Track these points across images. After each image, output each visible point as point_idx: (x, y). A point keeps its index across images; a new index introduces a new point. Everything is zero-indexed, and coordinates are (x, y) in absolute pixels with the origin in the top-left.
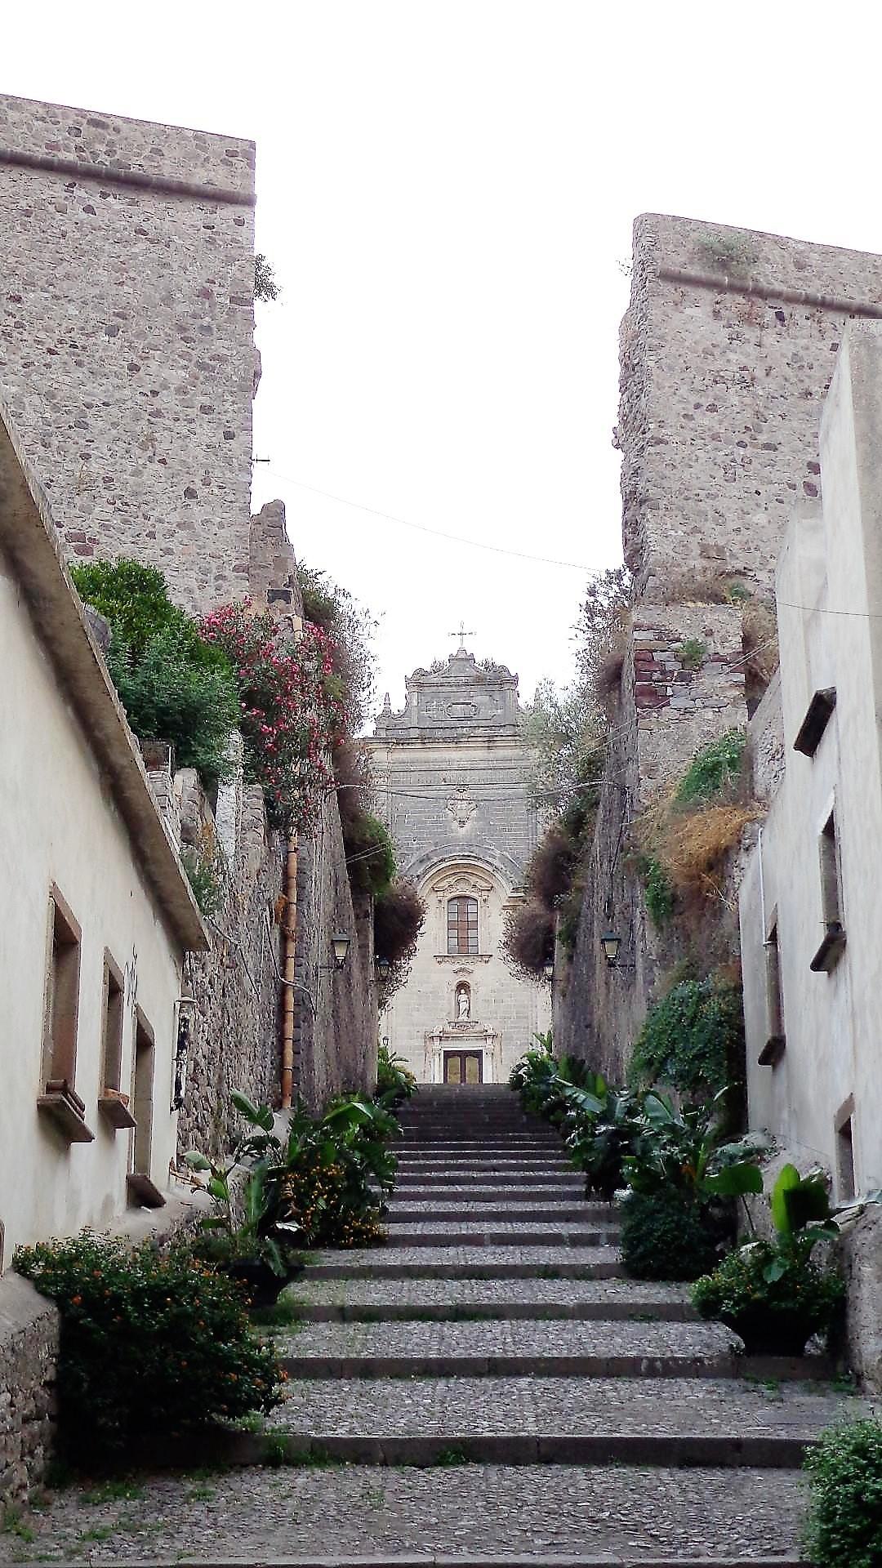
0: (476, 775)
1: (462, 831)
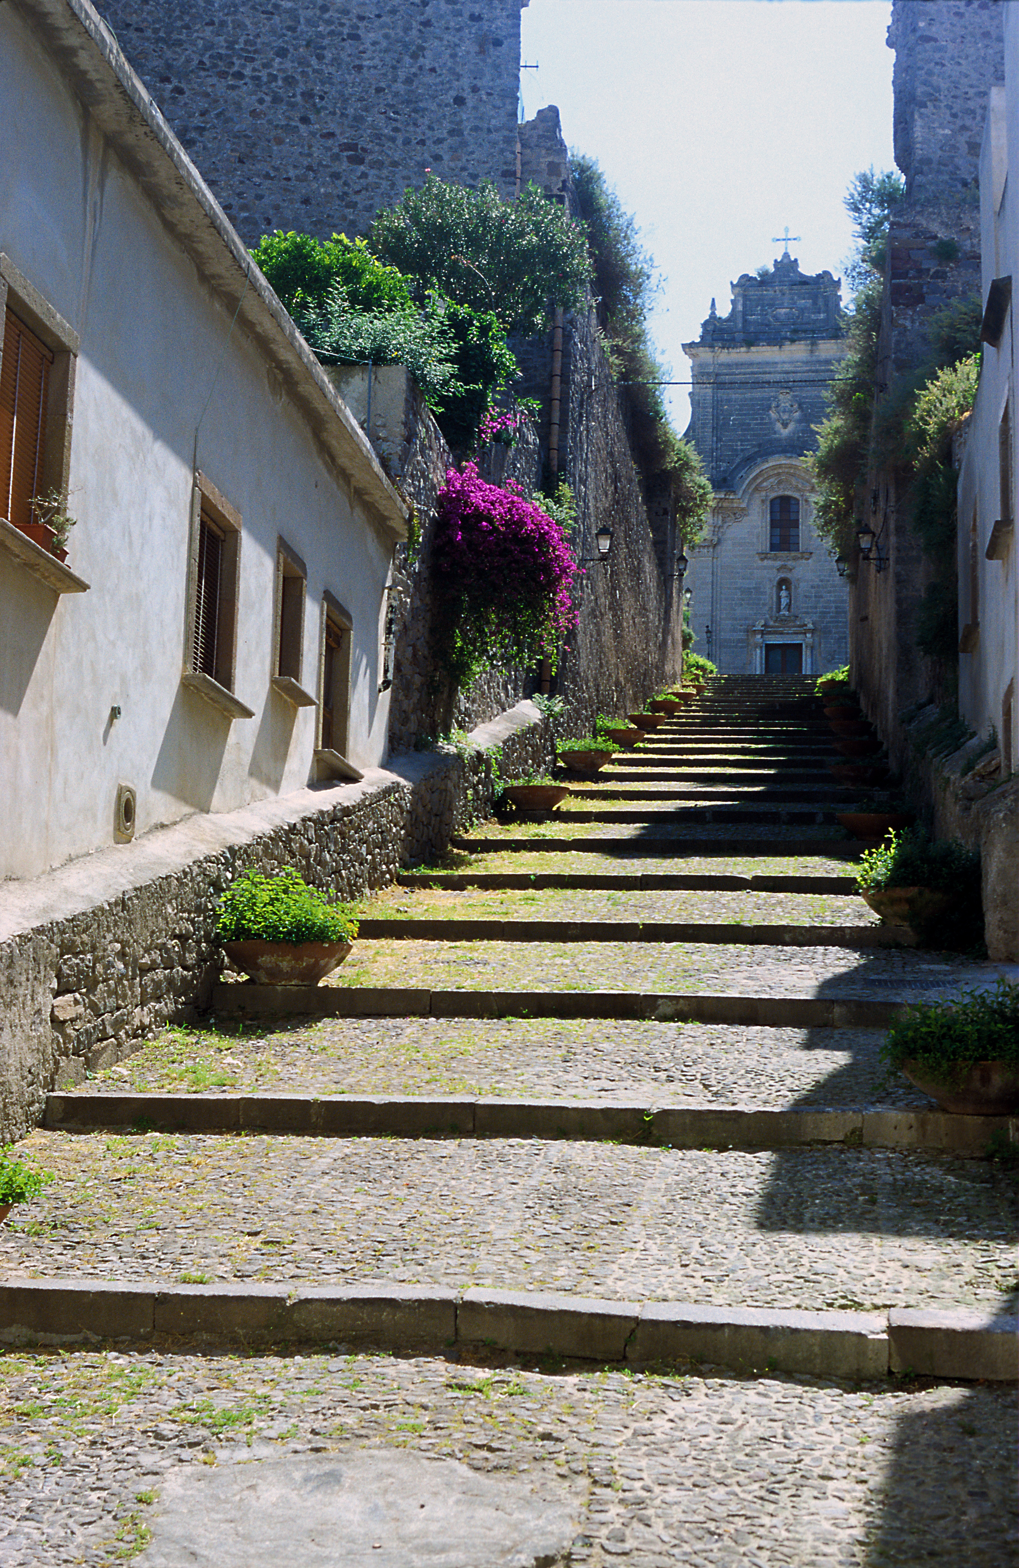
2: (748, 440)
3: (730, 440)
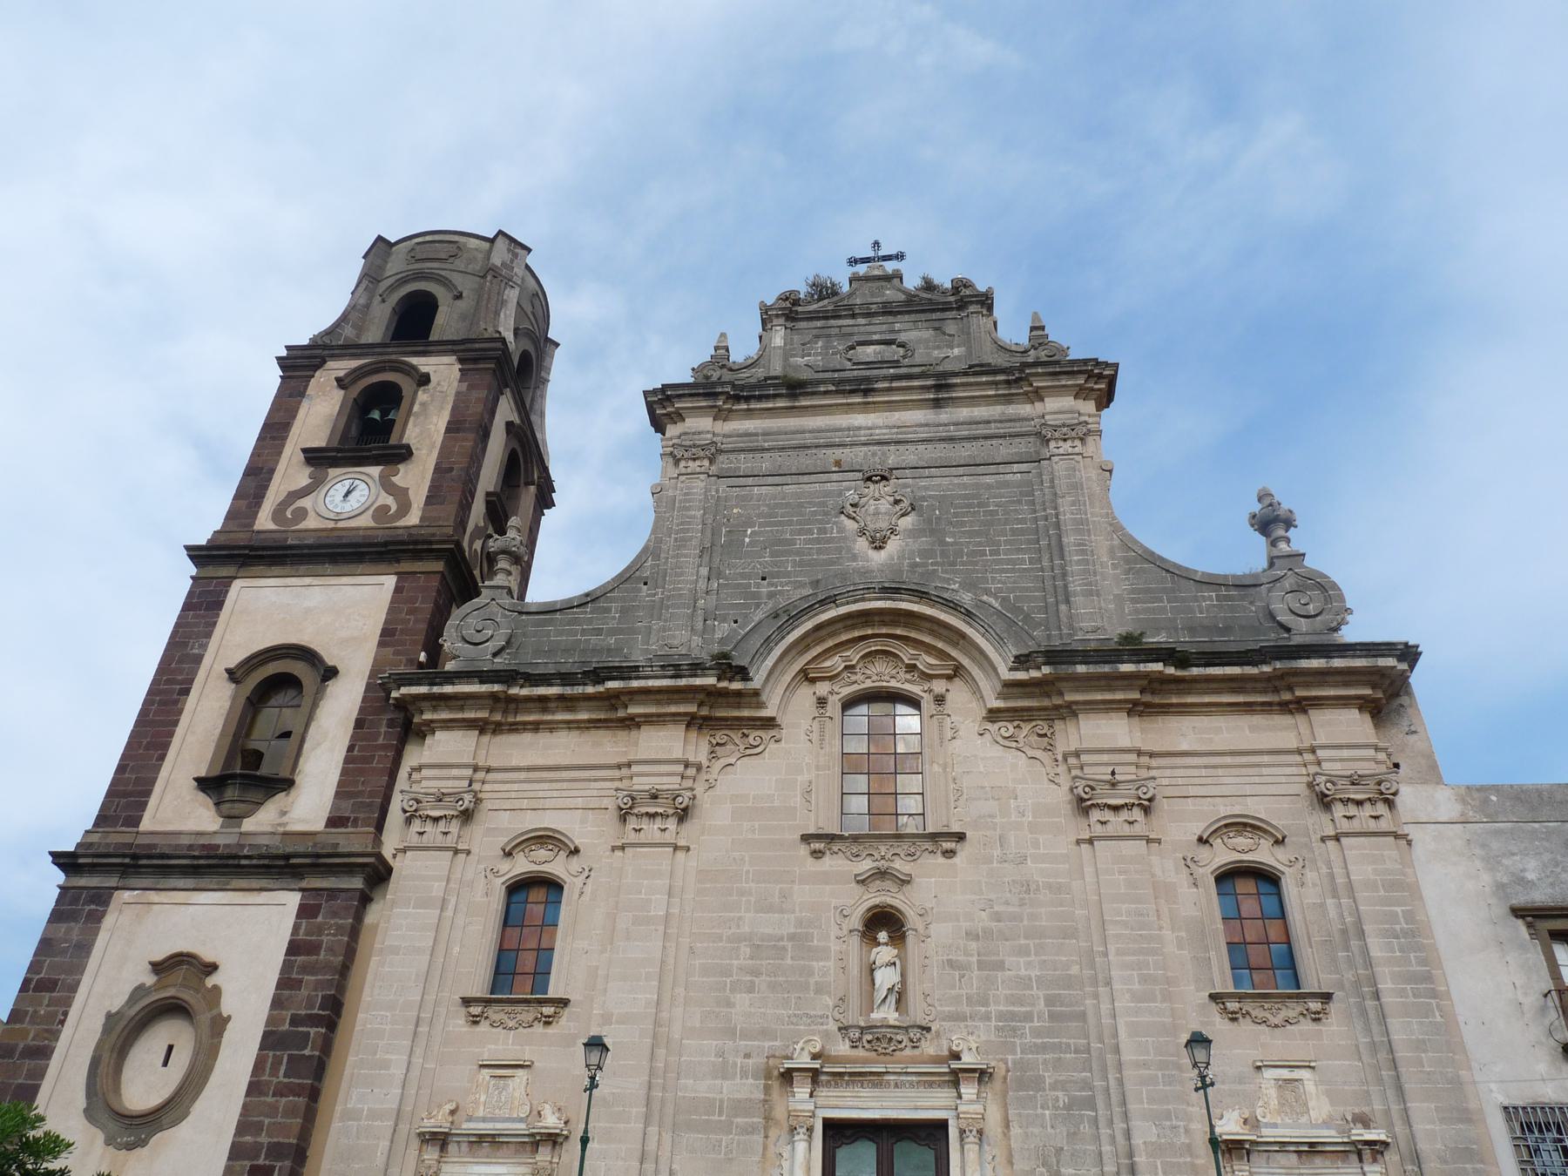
0: (910, 455)
1: (878, 558)
2: (788, 574)
3: (743, 576)
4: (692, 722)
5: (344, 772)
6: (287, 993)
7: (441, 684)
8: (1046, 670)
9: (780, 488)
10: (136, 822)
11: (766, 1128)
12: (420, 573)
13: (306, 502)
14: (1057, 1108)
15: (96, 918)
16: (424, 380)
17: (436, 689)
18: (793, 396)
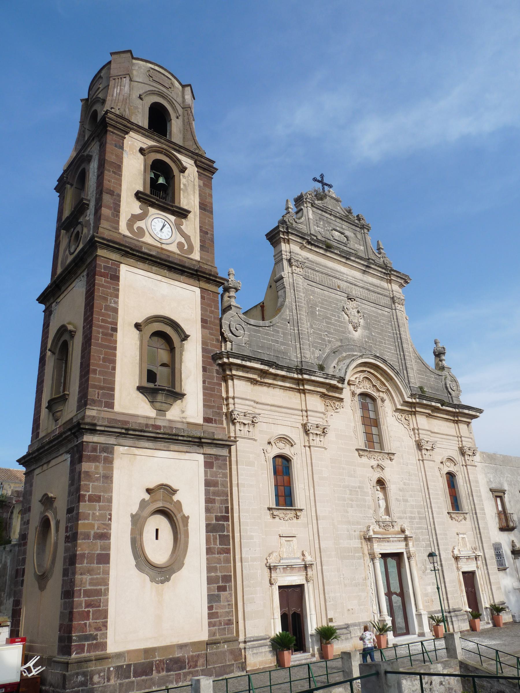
4: (323, 396)
5: (204, 394)
6: (210, 505)
7: (246, 361)
8: (418, 400)
9: (323, 291)
10: (111, 405)
11: (363, 557)
12: (210, 291)
13: (141, 224)
14: (423, 547)
15: (109, 461)
16: (183, 170)
17: (244, 363)
18: (326, 250)
